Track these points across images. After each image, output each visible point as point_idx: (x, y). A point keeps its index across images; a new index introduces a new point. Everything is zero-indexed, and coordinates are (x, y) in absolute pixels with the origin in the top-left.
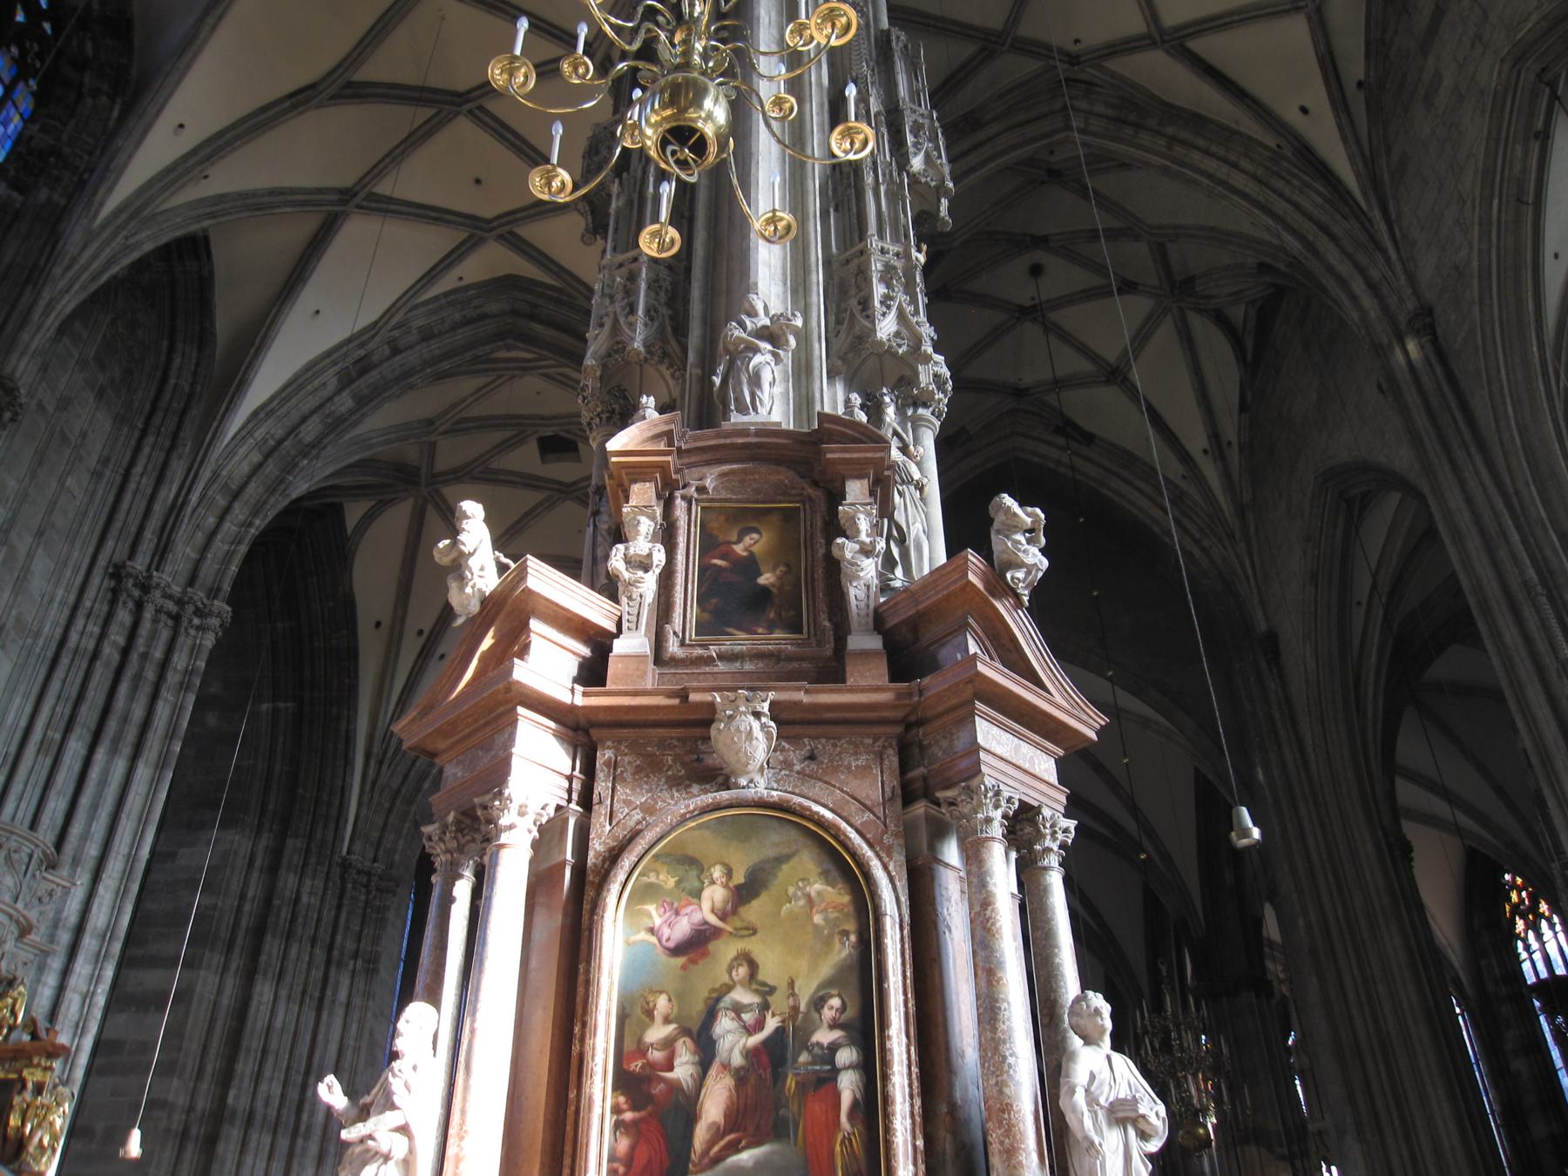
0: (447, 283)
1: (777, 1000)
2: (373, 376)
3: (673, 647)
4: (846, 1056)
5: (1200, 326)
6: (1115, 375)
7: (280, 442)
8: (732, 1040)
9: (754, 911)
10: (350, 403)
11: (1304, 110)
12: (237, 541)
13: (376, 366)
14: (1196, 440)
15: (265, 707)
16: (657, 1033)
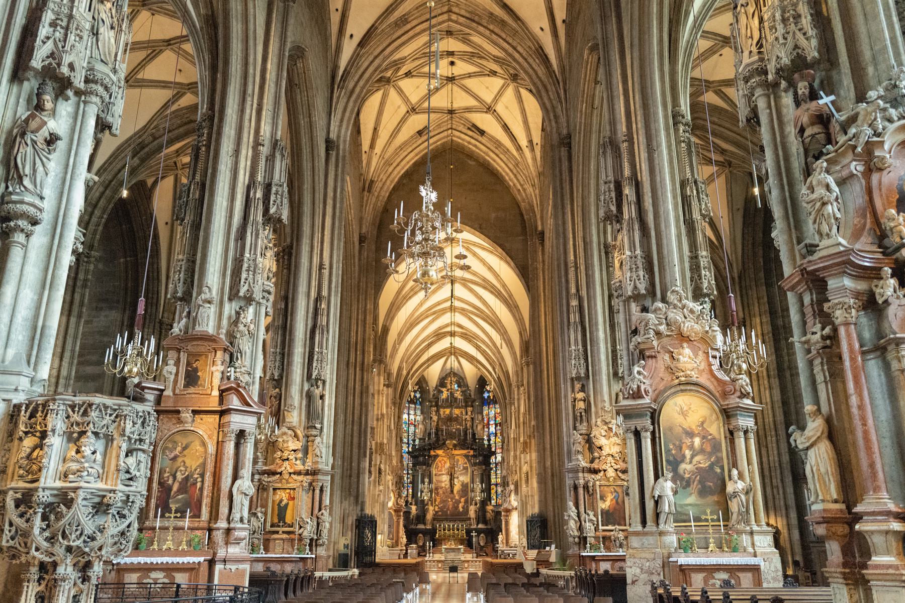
0: (175, 107)
1: (189, 470)
2: (146, 150)
3: (177, 391)
4: (199, 480)
5: (524, 93)
6: (489, 109)
7: (111, 182)
8: (179, 476)
9: (185, 452)
10: (138, 161)
11: (542, 29)
12: (98, 225)
13: (147, 145)
14: (524, 143)
15: (122, 260)
16: (166, 475)
